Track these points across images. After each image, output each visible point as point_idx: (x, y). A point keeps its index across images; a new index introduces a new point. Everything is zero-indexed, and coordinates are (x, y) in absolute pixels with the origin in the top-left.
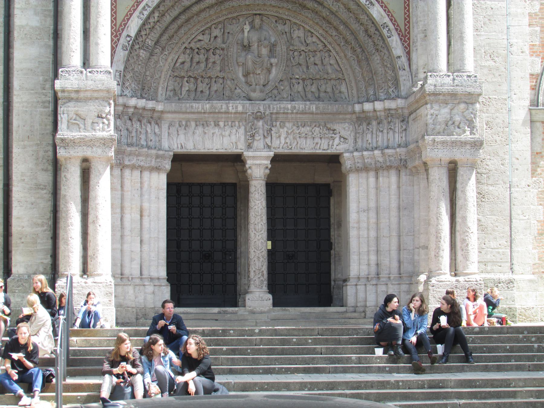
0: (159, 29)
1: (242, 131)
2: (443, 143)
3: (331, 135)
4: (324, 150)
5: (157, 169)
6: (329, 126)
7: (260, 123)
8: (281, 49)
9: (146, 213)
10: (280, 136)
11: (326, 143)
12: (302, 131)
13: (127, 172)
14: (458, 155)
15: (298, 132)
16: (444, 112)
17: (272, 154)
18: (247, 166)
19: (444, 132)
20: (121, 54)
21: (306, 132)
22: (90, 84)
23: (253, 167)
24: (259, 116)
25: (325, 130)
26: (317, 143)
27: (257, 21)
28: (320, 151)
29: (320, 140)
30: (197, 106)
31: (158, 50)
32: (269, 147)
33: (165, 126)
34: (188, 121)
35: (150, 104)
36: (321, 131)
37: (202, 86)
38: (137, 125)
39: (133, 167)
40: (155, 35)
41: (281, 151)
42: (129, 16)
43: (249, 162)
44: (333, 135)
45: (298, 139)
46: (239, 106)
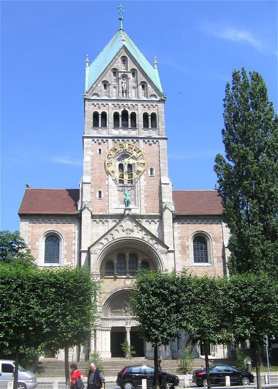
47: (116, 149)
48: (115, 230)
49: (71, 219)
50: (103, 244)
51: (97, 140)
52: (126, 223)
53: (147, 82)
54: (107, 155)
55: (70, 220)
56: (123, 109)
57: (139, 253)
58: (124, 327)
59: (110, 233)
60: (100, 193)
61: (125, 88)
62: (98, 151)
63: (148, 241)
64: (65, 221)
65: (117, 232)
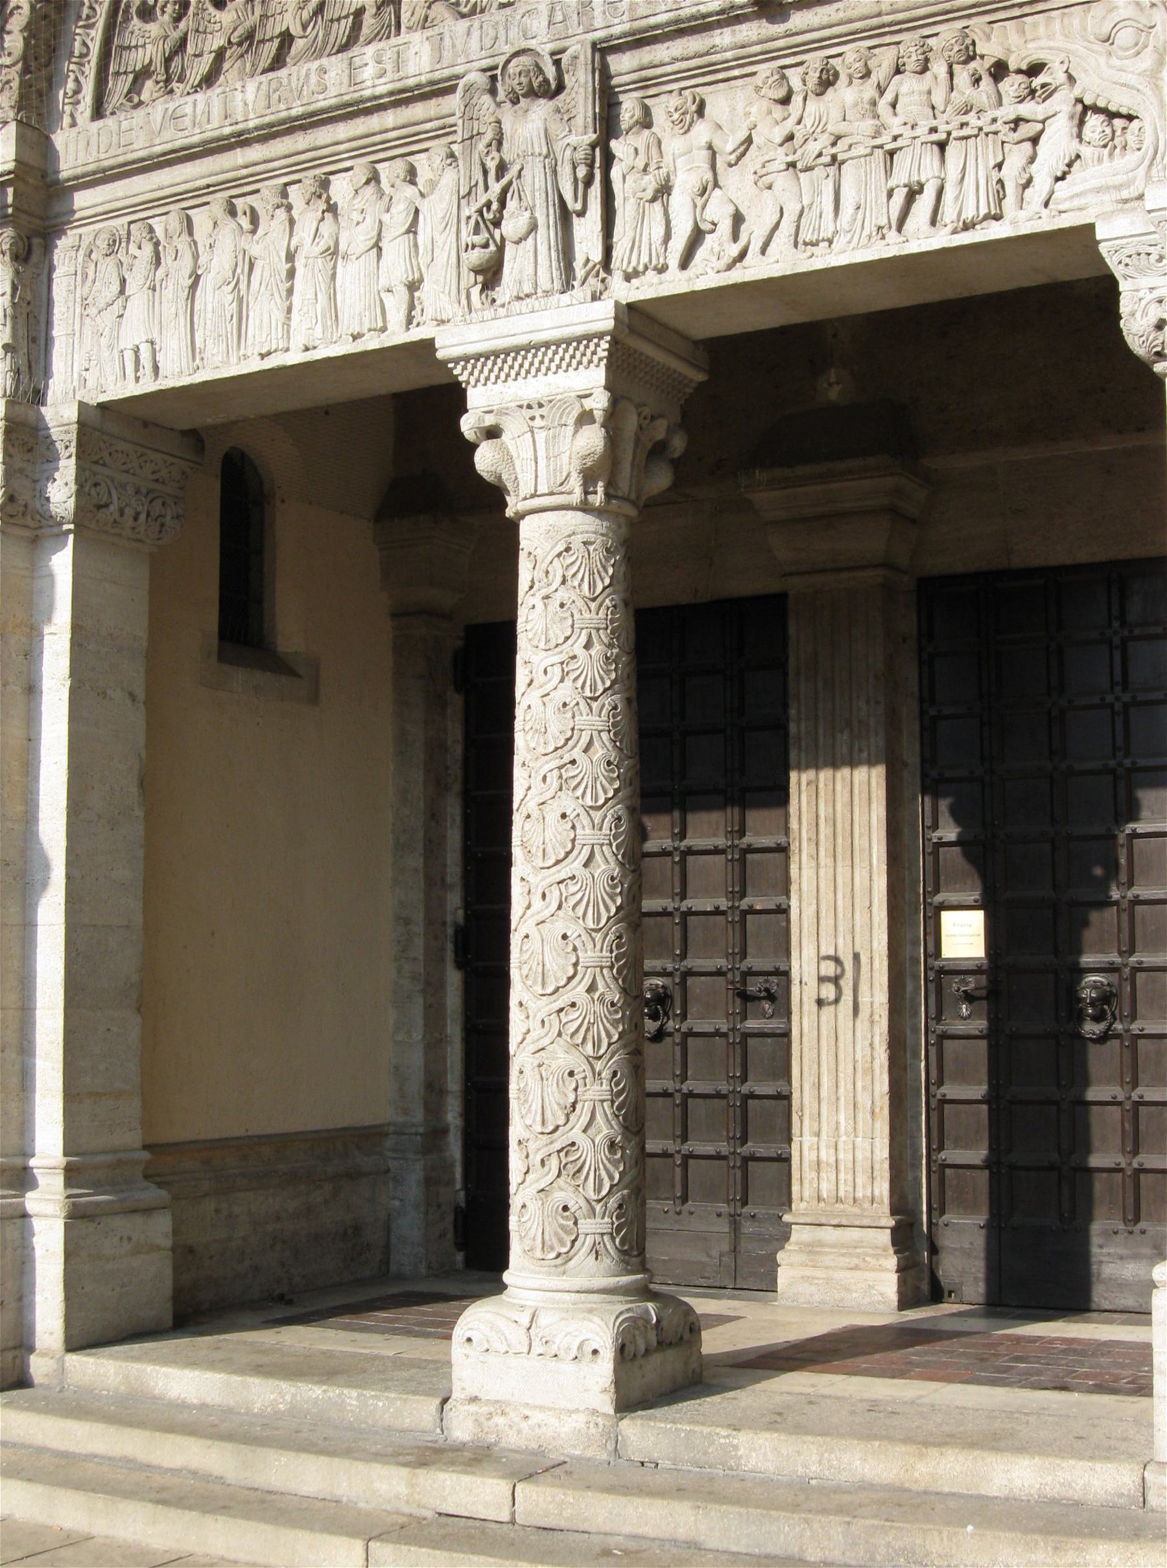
3: (1009, 111)
4: (967, 227)
6: (991, 49)
10: (664, 191)
11: (980, 172)
12: (808, 121)
15: (779, 134)
17: (602, 316)
18: (468, 425)
21: (834, 127)
23: (512, 429)
25: (963, 76)
26: (913, 193)
28: (941, 239)
29: (931, 157)
36: (938, 98)
44: (1027, 109)
45: (782, 181)
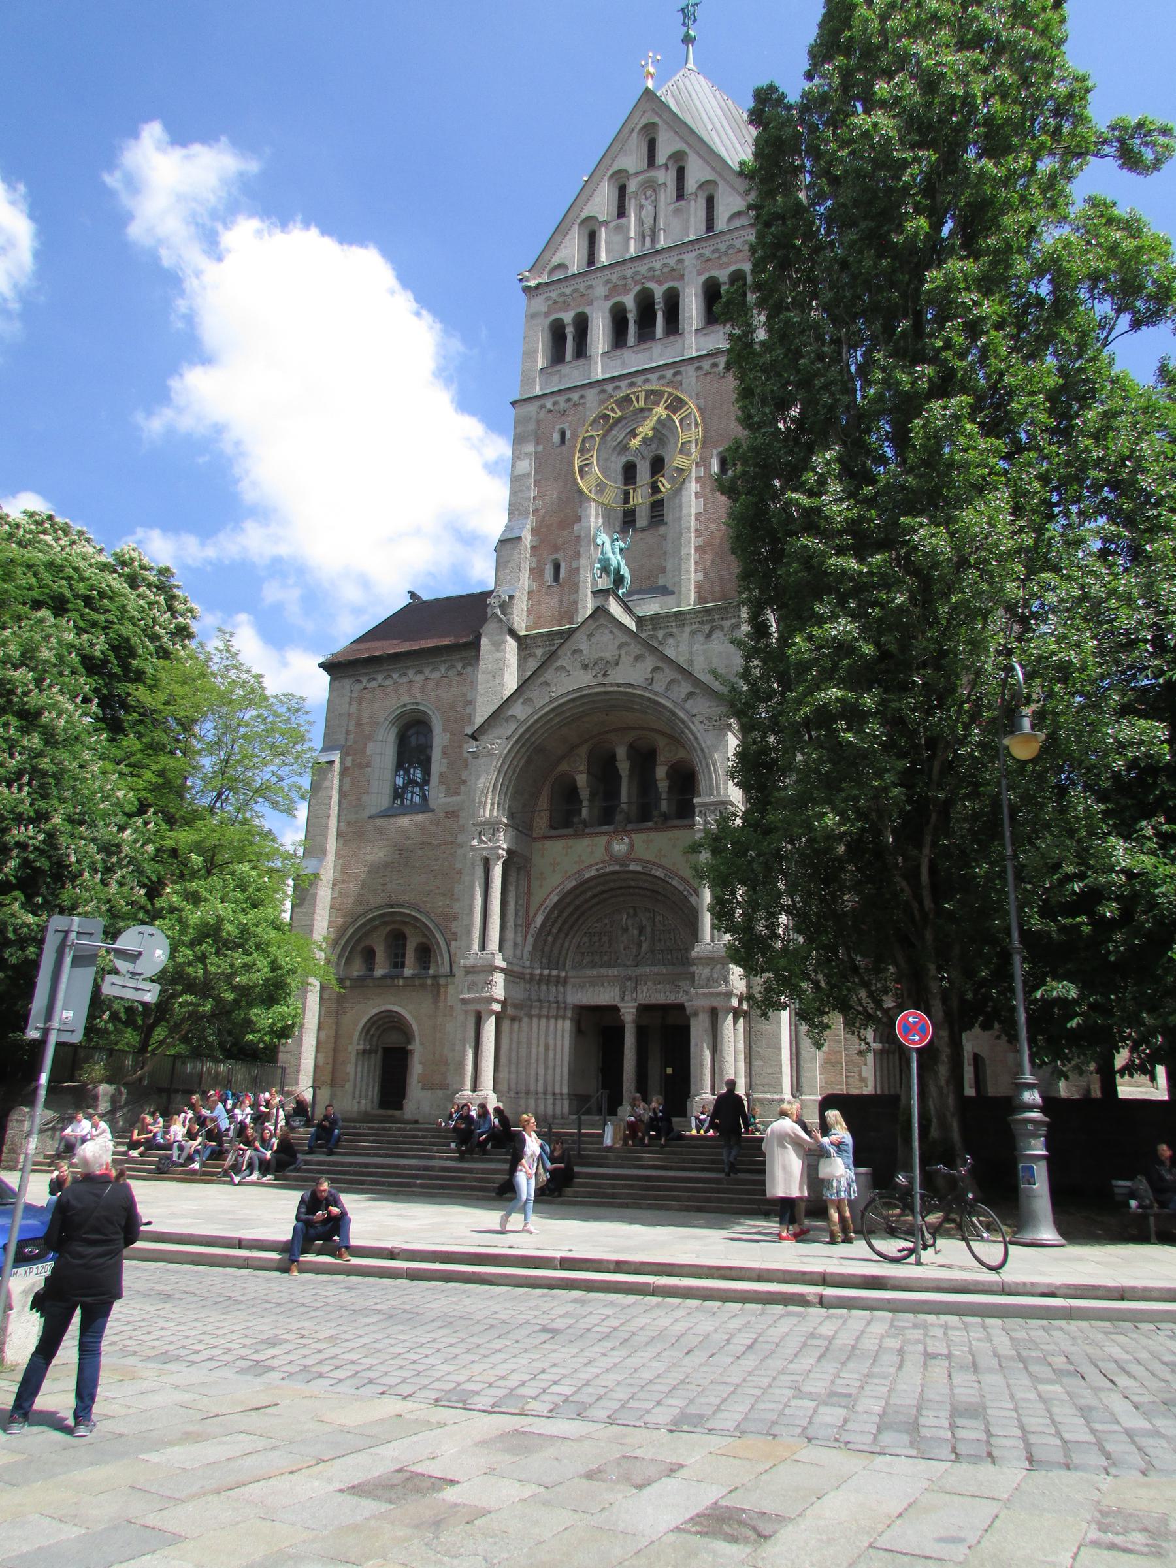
0: (560, 921)
1: (618, 989)
2: (704, 994)
5: (564, 1018)
7: (629, 983)
8: (649, 929)
9: (551, 1047)
13: (535, 1020)
14: (715, 1002)
16: (706, 972)
19: (706, 986)
20: (530, 940)
22: (480, 962)
24: (630, 978)
27: (631, 911)
30: (589, 972)
31: (562, 935)
32: (636, 1000)
33: (569, 987)
34: (584, 983)
35: (554, 973)
37: (597, 958)
38: (544, 987)
39: (539, 1017)
40: (557, 926)
41: (643, 1002)
42: (536, 914)
43: (622, 1011)
46: (615, 971)
47: (606, 417)
48: (557, 669)
49: (461, 659)
50: (518, 720)
51: (555, 403)
52: (594, 639)
53: (718, 179)
54: (580, 440)
55: (459, 666)
56: (638, 288)
57: (661, 742)
58: (614, 1009)
59: (542, 679)
60: (557, 568)
61: (649, 222)
62: (556, 437)
63: (667, 689)
64: (447, 670)
65: (564, 675)
